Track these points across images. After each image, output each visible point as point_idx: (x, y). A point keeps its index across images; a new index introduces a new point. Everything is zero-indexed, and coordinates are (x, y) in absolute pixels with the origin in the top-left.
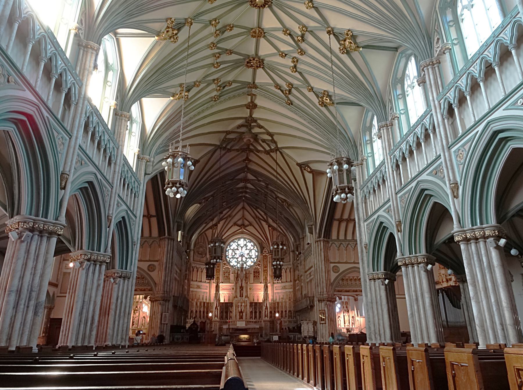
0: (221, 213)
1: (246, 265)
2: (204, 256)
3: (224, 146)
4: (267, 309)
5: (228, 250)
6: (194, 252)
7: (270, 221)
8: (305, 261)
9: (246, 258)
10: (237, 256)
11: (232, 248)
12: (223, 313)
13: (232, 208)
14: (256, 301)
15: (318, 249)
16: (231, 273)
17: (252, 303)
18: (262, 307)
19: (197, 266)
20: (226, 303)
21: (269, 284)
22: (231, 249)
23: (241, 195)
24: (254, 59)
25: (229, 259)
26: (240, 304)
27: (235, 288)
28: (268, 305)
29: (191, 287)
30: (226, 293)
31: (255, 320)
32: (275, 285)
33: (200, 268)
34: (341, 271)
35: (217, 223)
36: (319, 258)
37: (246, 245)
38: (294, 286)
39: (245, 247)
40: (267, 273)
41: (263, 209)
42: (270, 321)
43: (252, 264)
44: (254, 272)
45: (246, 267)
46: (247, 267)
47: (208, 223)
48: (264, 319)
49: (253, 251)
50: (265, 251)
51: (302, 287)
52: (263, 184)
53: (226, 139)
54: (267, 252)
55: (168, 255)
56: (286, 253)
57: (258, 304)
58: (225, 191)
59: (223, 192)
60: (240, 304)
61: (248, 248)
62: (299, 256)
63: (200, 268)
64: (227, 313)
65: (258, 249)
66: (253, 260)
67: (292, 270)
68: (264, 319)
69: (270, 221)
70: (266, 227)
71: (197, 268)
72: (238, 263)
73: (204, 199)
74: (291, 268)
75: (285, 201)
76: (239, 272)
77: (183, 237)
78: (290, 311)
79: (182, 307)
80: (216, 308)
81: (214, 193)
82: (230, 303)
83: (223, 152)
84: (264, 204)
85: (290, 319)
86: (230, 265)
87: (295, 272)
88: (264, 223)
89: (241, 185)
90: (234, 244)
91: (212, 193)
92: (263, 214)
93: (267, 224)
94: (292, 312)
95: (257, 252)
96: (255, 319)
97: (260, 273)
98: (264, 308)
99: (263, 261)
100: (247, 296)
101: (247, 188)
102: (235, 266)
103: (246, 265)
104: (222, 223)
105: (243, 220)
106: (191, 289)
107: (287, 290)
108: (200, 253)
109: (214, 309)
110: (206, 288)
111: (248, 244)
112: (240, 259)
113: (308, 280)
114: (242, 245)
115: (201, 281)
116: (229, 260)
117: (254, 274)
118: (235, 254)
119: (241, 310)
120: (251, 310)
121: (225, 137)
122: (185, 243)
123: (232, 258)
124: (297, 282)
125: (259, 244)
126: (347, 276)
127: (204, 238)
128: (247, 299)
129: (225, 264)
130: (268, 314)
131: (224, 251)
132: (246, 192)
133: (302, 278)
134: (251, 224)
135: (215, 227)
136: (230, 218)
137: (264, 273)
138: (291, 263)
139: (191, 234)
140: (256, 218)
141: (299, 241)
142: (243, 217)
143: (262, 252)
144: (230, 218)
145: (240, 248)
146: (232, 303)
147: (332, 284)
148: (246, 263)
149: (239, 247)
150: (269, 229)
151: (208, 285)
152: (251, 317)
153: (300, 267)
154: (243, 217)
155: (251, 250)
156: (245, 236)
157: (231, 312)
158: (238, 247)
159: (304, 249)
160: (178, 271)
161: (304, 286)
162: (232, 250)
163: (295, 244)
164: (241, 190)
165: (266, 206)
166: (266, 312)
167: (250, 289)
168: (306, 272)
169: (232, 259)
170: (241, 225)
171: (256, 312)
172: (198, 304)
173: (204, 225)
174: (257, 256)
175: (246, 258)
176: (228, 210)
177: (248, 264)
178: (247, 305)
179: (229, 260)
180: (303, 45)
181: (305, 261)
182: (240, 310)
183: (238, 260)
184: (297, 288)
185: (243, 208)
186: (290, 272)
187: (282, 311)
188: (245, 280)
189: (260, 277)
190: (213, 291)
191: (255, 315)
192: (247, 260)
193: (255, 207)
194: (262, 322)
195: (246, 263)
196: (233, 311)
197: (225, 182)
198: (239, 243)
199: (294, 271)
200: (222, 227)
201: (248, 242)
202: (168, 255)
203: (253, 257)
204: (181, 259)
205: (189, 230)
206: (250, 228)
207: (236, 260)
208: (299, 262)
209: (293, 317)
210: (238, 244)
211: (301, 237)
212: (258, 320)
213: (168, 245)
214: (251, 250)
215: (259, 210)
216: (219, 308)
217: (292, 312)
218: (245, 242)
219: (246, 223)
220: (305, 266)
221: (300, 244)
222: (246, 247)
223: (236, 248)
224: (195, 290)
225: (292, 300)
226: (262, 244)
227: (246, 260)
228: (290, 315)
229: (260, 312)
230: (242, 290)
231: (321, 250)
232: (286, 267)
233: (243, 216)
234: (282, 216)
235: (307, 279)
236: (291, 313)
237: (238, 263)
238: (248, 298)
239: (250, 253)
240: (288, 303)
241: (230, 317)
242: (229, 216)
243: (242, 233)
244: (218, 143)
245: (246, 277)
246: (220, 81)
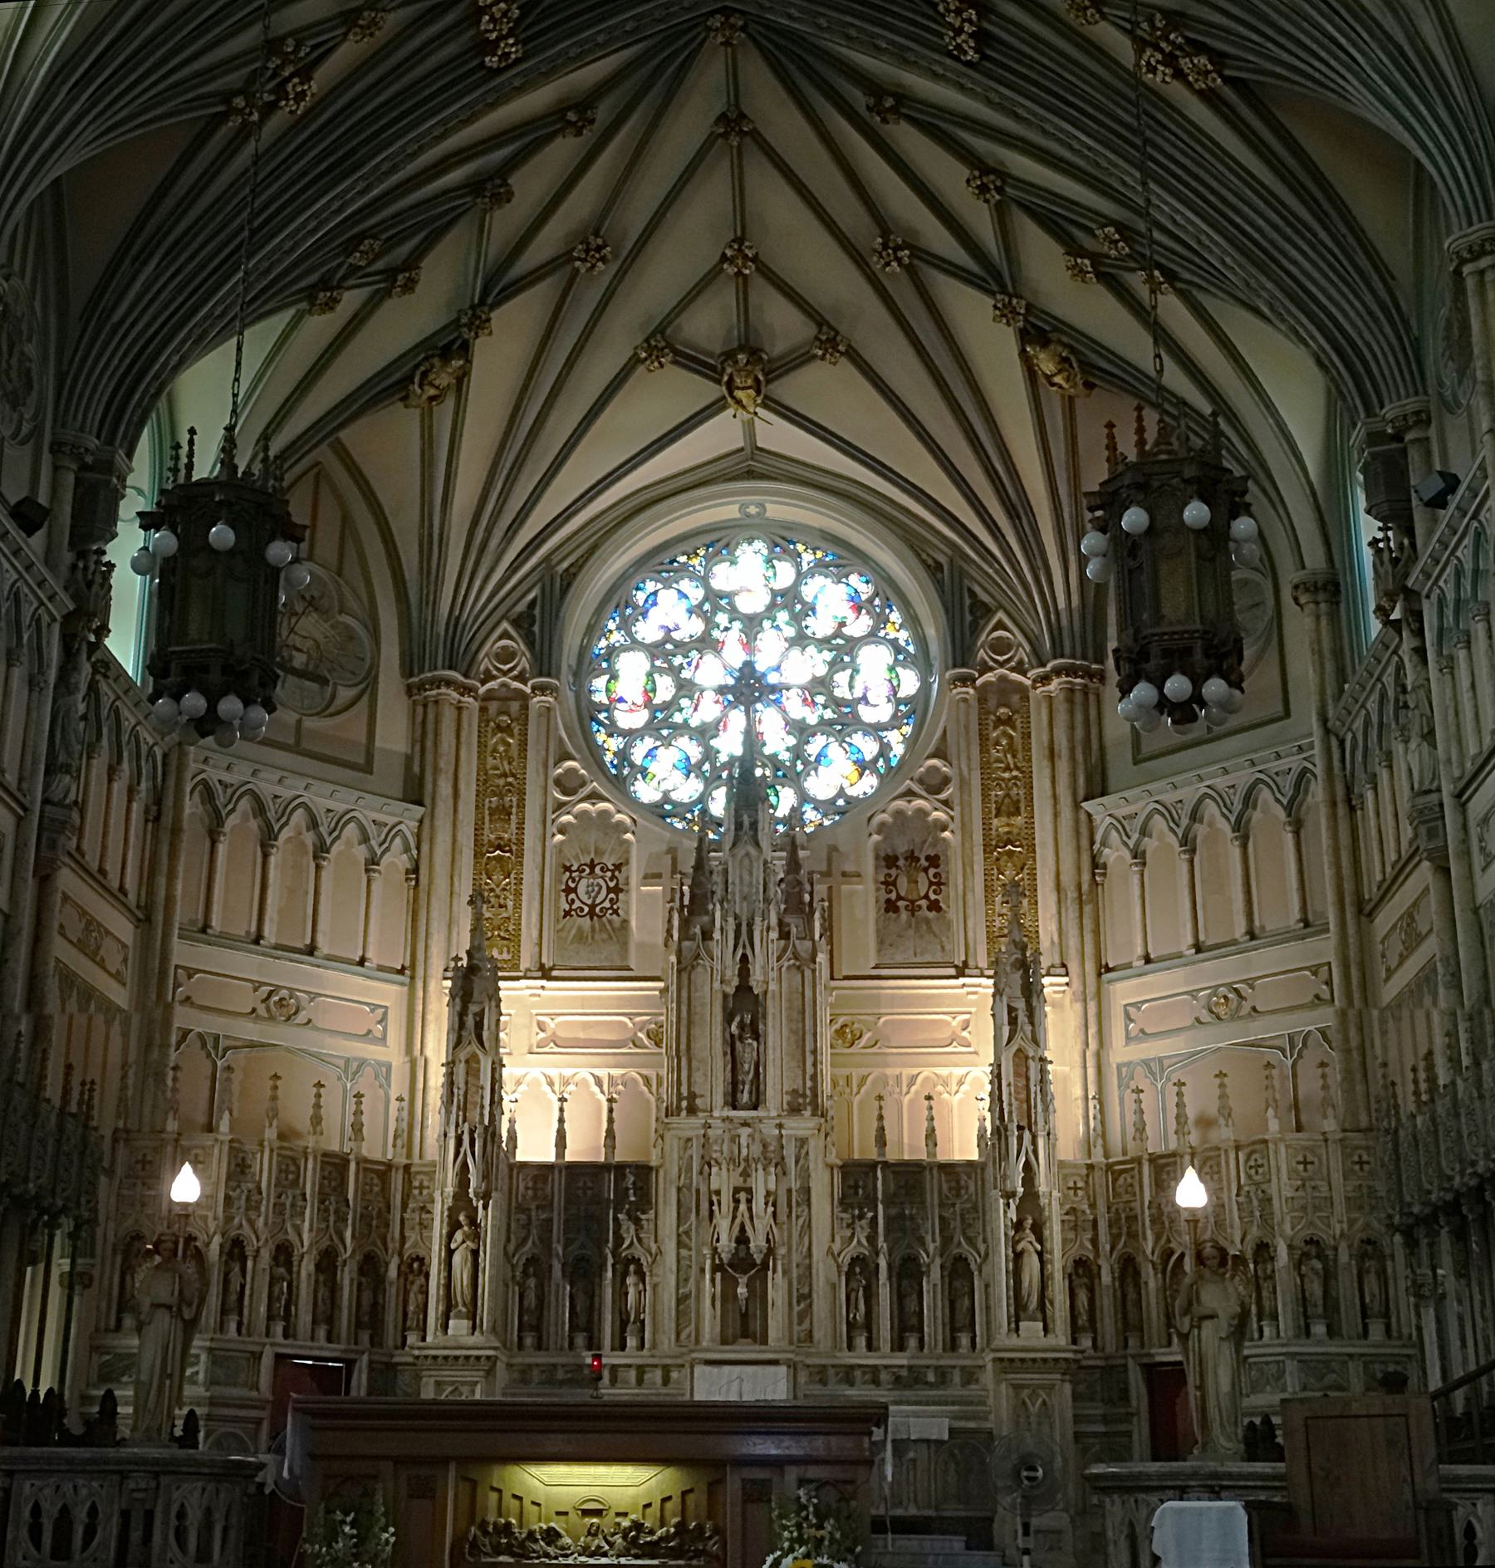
1: (804, 797)
2: (345, 694)
4: (1038, 1230)
11: (647, 630)
12: (543, 1276)
14: (907, 1146)
16: (634, 872)
17: (873, 1166)
18: (977, 1212)
19: (266, 787)
20: (575, 1170)
21: (1051, 985)
22: (635, 644)
25: (614, 744)
26: (723, 1180)
27: (668, 1035)
28: (1042, 1186)
30: (584, 1074)
31: (901, 1360)
32: (1122, 992)
33: (299, 816)
39: (783, 616)
40: (1026, 864)
42: (1073, 1369)
43: (868, 784)
44: (890, 861)
45: (796, 814)
46: (810, 814)
48: (1003, 1338)
49: (874, 661)
50: (1000, 647)
54: (1023, 653)
57: (933, 1188)
60: (723, 1180)
61: (820, 626)
63: (299, 816)
64: (583, 1272)
65: (921, 640)
66: (869, 748)
68: (1003, 1338)
71: (260, 809)
72: (711, 782)
74: (1303, 778)
78: (1311, 1249)
80: (462, 1212)
82: (620, 1168)
85: (1320, 1343)
86: (633, 803)
90: (667, 597)
95: (909, 661)
96: (899, 1345)
97: (954, 868)
98: (1003, 1215)
99: (983, 738)
100: (805, 1101)
102: (680, 810)
106: (182, 1017)
109: (438, 1228)
114: (753, 602)
115: (311, 950)
116: (623, 755)
117: (889, 884)
119: (742, 1240)
120: (859, 1245)
125: (934, 569)
127: (346, 520)
128: (802, 1125)
129: (569, 785)
137: (994, 865)
138: (1306, 717)
143: (961, 651)
146: (643, 1171)
152: (861, 1327)
155: (853, 644)
156: (782, 508)
157: (629, 1266)
162: (654, 650)
166: (1032, 1264)
167: (846, 1035)
169: (649, 742)
171: (908, 1272)
172: (264, 1168)
174: (913, 709)
175: (801, 731)
177: (821, 786)
178: (806, 1191)
179: (623, 755)
182: (726, 1244)
189: (953, 913)
191: (899, 1297)
194: (988, 1377)
195: (793, 778)
198: (717, 584)
201: (820, 567)
203: (867, 714)
207: (695, 752)
209: (1349, 1314)
210: (713, 596)
212: (933, 1356)
214: (843, 649)
216: (489, 1218)
218: (785, 574)
222: (796, 619)
223: (694, 627)
225: (1330, 1125)
226: (959, 574)
227: (797, 752)
229: (959, 1272)
230: (754, 1031)
232: (1243, 777)
238: (818, 1111)
239: (842, 678)
240: (1282, 1161)
241: (622, 1323)
245: (797, 905)
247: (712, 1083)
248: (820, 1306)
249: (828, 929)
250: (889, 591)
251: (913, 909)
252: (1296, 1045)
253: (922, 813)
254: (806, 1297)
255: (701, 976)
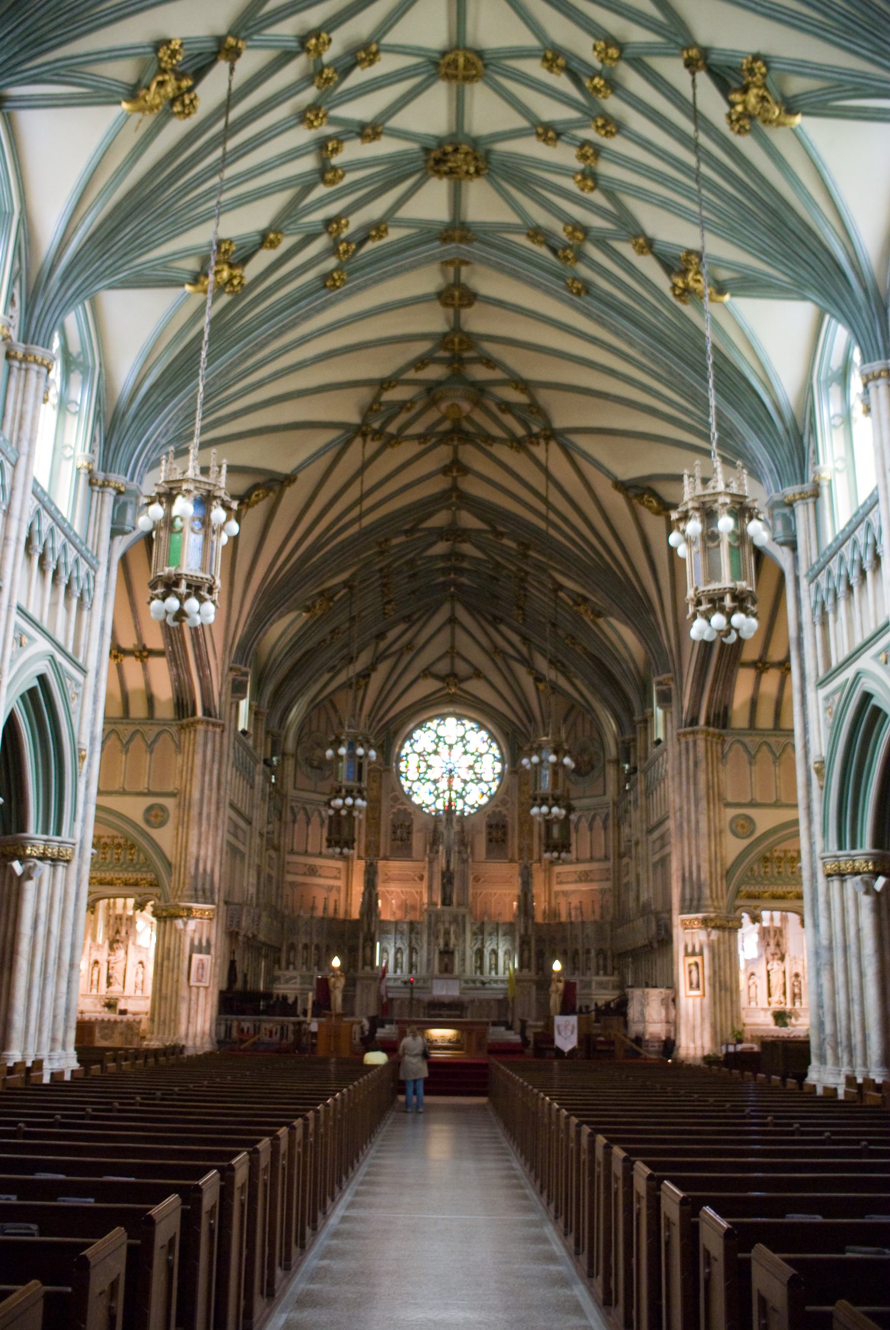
0: (381, 636)
1: (465, 804)
3: (376, 425)
5: (407, 755)
6: (297, 763)
7: (542, 664)
8: (647, 797)
9: (465, 782)
10: (432, 775)
11: (418, 748)
13: (418, 619)
15: (688, 760)
23: (442, 579)
24: (456, 150)
25: (408, 784)
29: (289, 872)
34: (757, 834)
35: (367, 668)
36: (688, 790)
37: (463, 738)
38: (617, 875)
41: (516, 624)
45: (462, 811)
47: (340, 671)
51: (638, 876)
52: (513, 545)
53: (381, 404)
55: (207, 778)
56: (593, 767)
58: (388, 566)
59: (381, 570)
61: (470, 748)
62: (633, 777)
65: (501, 753)
67: (611, 822)
69: (542, 664)
70: (527, 682)
72: (438, 797)
73: (321, 594)
75: (585, 599)
76: (442, 828)
77: (255, 713)
79: (254, 936)
81: (353, 575)
83: (372, 446)
84: (520, 608)
87: (619, 827)
88: (521, 671)
89: (440, 548)
91: (344, 576)
92: (515, 639)
93: (530, 673)
94: (609, 953)
95: (499, 761)
101: (463, 557)
103: (465, 804)
104: (383, 668)
105: (452, 658)
107: (595, 886)
108: (315, 763)
110: (335, 873)
111: (470, 736)
112: (443, 785)
113: (657, 857)
117: (489, 833)
118: (429, 767)
121: (376, 400)
122: (261, 735)
123: (419, 780)
124: (625, 860)
126: (778, 848)
128: (463, 910)
130: (530, 957)
131: (395, 758)
132: (460, 571)
133: (640, 847)
134: (478, 674)
135: (362, 682)
136: (411, 654)
139: (283, 704)
140: (494, 652)
141: (634, 732)
142: (452, 652)
144: (411, 654)
145: (443, 749)
147: (728, 874)
148: (462, 797)
149: (441, 744)
150: (537, 689)
151: (340, 864)
153: (635, 816)
154: (452, 652)
155: (481, 755)
158: (437, 745)
159: (646, 758)
160: (242, 824)
161: (643, 876)
162: (420, 754)
163: (620, 739)
164: (441, 565)
165: (524, 614)
168: (650, 831)
169: (418, 784)
170: (448, 676)
173: (327, 676)
176: (402, 627)
177: (470, 800)
180: (613, 105)
181: (647, 797)
183: (437, 789)
184: (625, 880)
185: (453, 620)
186: (605, 828)
187: (576, 952)
188: (459, 852)
189: (509, 843)
190: (358, 888)
192: (468, 788)
193: (490, 618)
195: (462, 797)
196: (422, 948)
197: (386, 540)
199: (618, 826)
200: (385, 683)
202: (207, 778)
204: (252, 787)
205: (277, 694)
206: (476, 687)
207: (433, 788)
208: (631, 797)
210: (438, 737)
211: (637, 718)
213: (205, 745)
215: (503, 628)
217: (609, 953)
218: (460, 730)
219: (462, 668)
220: (648, 814)
221: (634, 740)
223: (431, 747)
224: (300, 879)
228: (601, 962)
231: (696, 764)
233: (452, 647)
234: (578, 649)
235: (654, 854)
236: (605, 958)
237: (438, 797)
242: (409, 646)
243: (452, 700)
244: (354, 418)
246: (347, 225)
247: (438, 899)
248: (468, 962)
249: (472, 852)
250: (492, 737)
251: (497, 841)
252: (603, 892)
253: (500, 812)
254: (463, 960)
255: (435, 864)
